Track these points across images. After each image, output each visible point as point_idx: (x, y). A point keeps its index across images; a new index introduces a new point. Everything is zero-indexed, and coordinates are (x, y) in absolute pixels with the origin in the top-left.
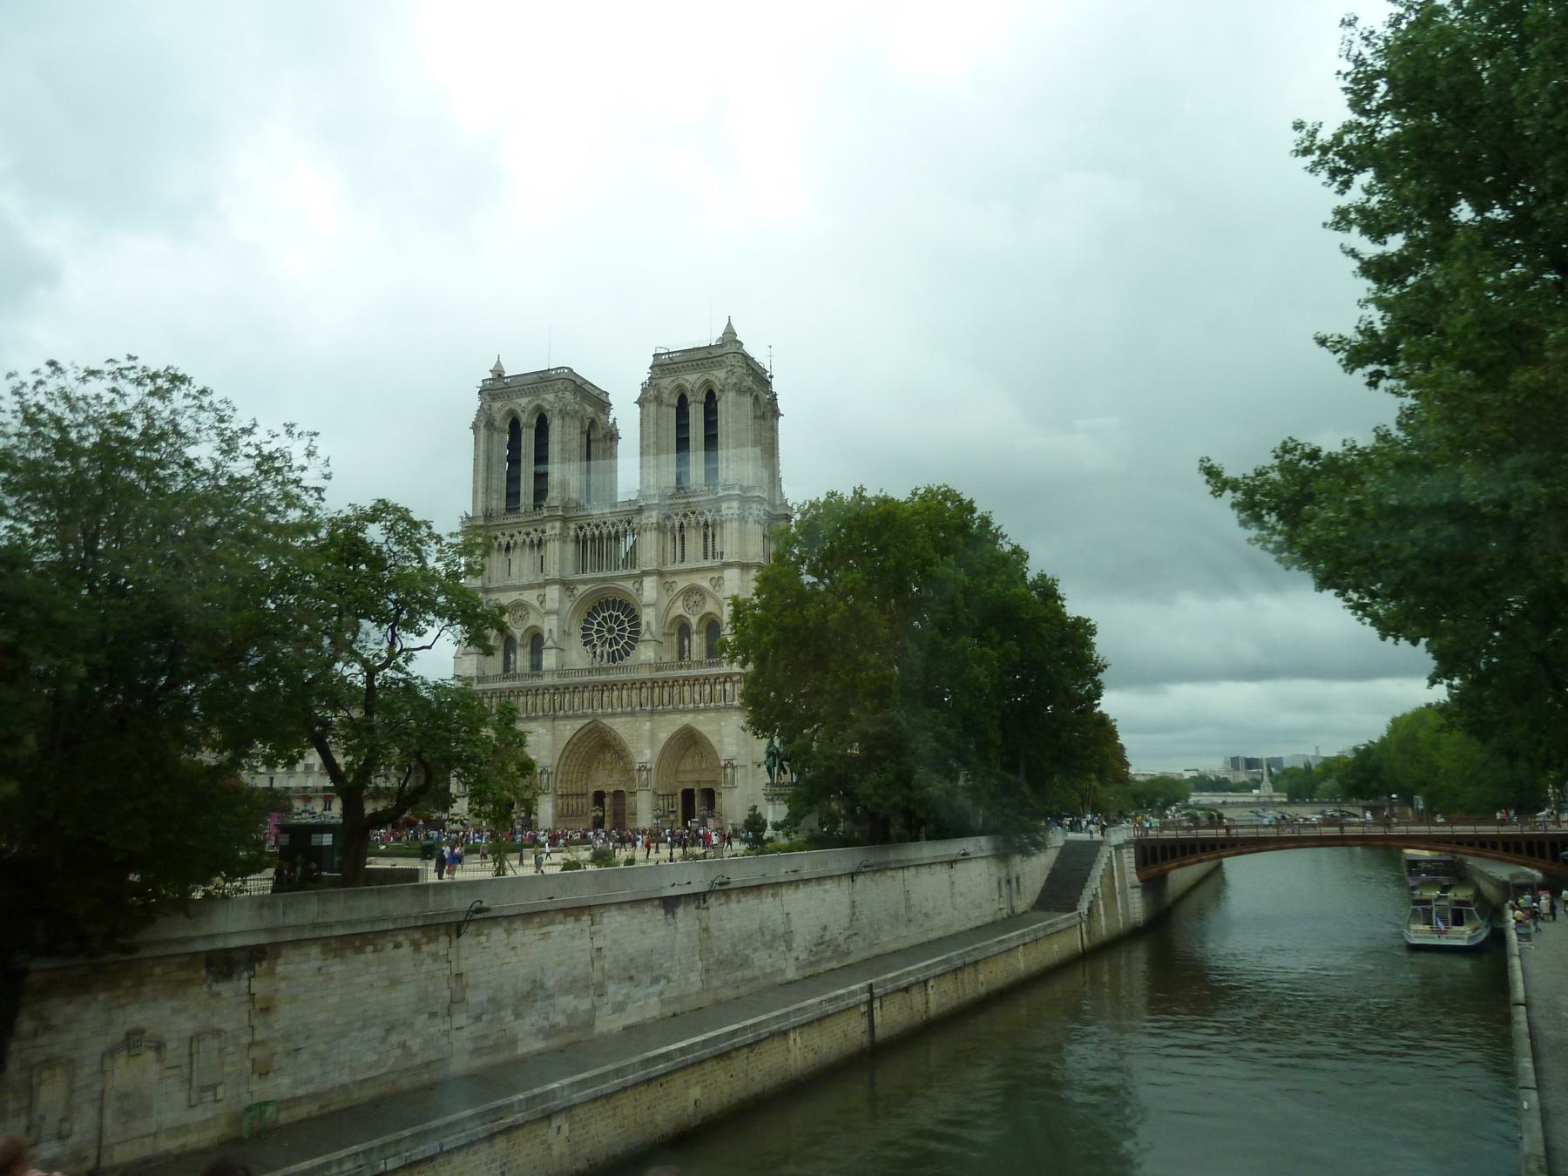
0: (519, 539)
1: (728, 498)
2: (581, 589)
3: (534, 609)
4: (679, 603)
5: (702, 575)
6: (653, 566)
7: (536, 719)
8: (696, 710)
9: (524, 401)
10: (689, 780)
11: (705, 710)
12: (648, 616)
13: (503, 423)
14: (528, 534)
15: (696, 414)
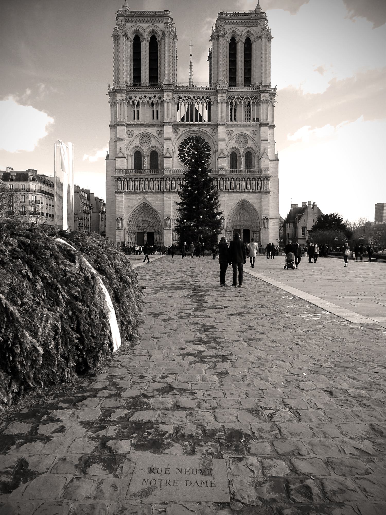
0: (146, 100)
1: (264, 92)
2: (181, 129)
3: (154, 137)
4: (234, 141)
5: (248, 129)
6: (223, 121)
7: (162, 192)
8: (249, 192)
9: (145, 26)
10: (247, 224)
11: (252, 193)
12: (221, 145)
13: (131, 37)
14: (150, 98)
15: (241, 48)
